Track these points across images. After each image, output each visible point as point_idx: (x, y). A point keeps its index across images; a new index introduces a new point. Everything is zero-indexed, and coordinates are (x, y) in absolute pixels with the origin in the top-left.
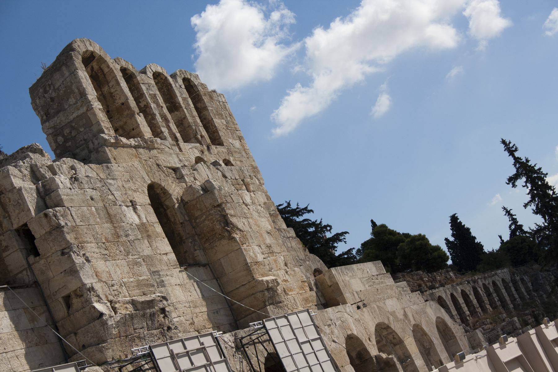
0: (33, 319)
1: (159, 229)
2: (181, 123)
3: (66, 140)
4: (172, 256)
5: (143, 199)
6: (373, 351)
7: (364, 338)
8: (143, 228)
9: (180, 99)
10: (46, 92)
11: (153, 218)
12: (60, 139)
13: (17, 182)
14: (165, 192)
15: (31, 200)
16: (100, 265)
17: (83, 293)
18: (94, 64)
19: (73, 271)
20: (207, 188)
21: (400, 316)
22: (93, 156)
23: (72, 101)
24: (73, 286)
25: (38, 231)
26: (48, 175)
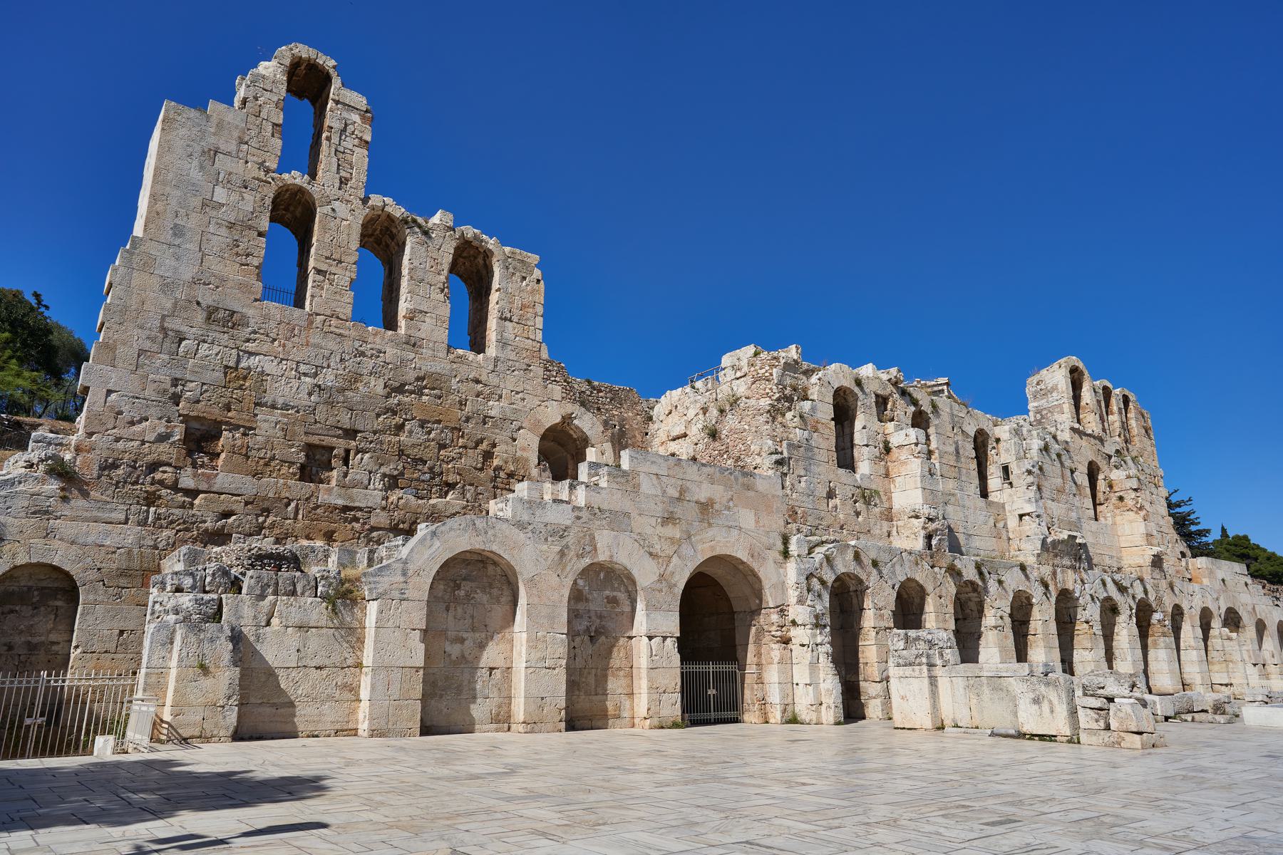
1: (1088, 491)
3: (1042, 417)
5: (1082, 470)
7: (1215, 613)
9: (1115, 408)
10: (1038, 384)
12: (1038, 416)
14: (1099, 469)
21: (1250, 608)
23: (1054, 394)
25: (1014, 468)
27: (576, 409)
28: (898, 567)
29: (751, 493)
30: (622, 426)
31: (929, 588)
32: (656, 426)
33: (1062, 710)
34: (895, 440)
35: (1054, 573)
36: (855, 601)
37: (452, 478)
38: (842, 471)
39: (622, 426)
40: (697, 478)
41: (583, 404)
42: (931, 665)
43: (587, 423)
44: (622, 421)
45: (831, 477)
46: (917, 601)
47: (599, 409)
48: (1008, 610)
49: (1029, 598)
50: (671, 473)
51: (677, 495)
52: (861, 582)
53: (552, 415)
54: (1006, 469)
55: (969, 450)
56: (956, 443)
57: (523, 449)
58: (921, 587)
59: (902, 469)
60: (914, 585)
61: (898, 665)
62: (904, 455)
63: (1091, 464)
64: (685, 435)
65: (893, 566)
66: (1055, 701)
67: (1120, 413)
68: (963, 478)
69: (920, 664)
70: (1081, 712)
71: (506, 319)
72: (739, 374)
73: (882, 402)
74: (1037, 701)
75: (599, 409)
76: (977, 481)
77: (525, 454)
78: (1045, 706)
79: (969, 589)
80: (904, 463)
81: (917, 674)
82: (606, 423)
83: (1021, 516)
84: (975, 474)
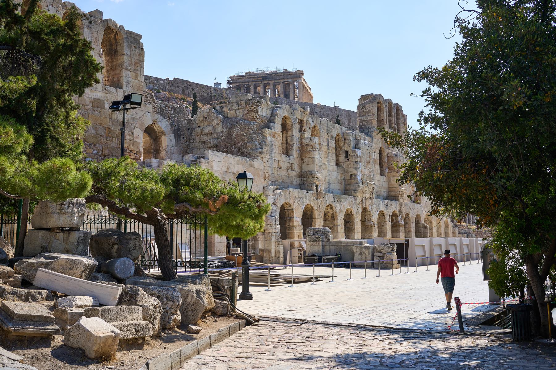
0: (341, 177)
2: (390, 121)
3: (363, 125)
4: (379, 171)
5: (378, 152)
6: (423, 221)
8: (375, 160)
9: (393, 114)
10: (362, 108)
11: (378, 158)
12: (361, 124)
13: (351, 138)
15: (352, 144)
16: (363, 170)
17: (356, 175)
18: (379, 105)
19: (356, 168)
20: (396, 155)
22: (369, 133)
23: (369, 114)
24: (354, 172)
26: (359, 138)
27: (158, 117)
28: (304, 199)
29: (253, 169)
30: (178, 125)
31: (315, 208)
32: (194, 126)
33: (369, 257)
34: (305, 142)
35: (362, 200)
36: (287, 213)
37: (106, 152)
38: (283, 156)
39: (178, 125)
40: (233, 162)
41: (162, 115)
42: (323, 241)
43: (163, 125)
44: (178, 122)
45: (279, 158)
46: (309, 213)
47: (169, 117)
48: (343, 217)
49: (351, 212)
50: (224, 160)
51: (226, 170)
52: (290, 206)
53: (148, 122)
54: (347, 153)
55: (333, 144)
56: (328, 141)
57: (137, 138)
58: (312, 207)
59: (307, 155)
60: (309, 206)
61: (310, 241)
62: (309, 149)
63: (381, 148)
64: (211, 133)
65: (303, 199)
66: (367, 254)
67: (395, 116)
68: (330, 158)
69: (319, 241)
70: (375, 257)
71: (128, 70)
72: (240, 107)
73: (301, 122)
74: (361, 254)
75: (169, 117)
76: (335, 158)
77: (137, 140)
78: (364, 256)
79: (329, 208)
80: (308, 152)
81: (317, 244)
82: (172, 124)
83: (351, 175)
84: (335, 155)
